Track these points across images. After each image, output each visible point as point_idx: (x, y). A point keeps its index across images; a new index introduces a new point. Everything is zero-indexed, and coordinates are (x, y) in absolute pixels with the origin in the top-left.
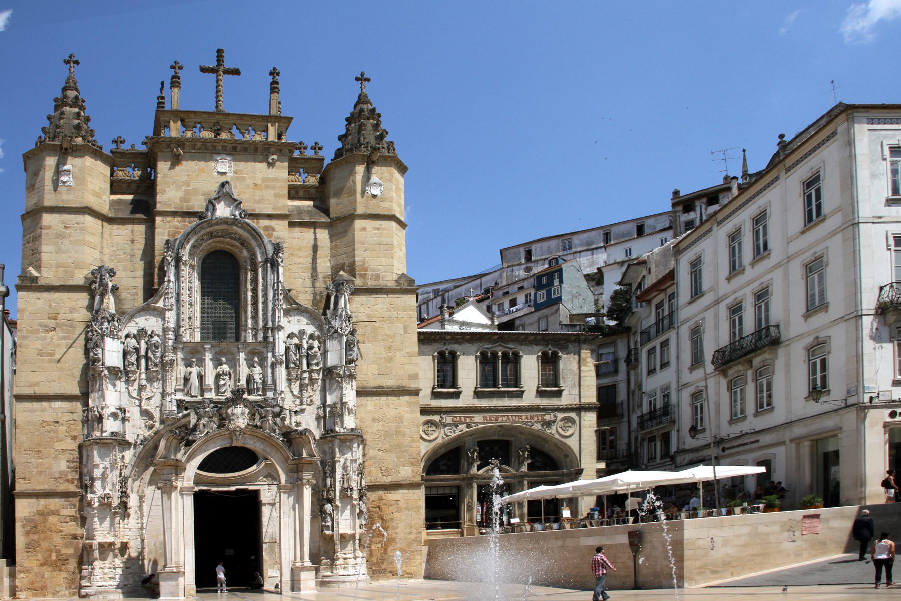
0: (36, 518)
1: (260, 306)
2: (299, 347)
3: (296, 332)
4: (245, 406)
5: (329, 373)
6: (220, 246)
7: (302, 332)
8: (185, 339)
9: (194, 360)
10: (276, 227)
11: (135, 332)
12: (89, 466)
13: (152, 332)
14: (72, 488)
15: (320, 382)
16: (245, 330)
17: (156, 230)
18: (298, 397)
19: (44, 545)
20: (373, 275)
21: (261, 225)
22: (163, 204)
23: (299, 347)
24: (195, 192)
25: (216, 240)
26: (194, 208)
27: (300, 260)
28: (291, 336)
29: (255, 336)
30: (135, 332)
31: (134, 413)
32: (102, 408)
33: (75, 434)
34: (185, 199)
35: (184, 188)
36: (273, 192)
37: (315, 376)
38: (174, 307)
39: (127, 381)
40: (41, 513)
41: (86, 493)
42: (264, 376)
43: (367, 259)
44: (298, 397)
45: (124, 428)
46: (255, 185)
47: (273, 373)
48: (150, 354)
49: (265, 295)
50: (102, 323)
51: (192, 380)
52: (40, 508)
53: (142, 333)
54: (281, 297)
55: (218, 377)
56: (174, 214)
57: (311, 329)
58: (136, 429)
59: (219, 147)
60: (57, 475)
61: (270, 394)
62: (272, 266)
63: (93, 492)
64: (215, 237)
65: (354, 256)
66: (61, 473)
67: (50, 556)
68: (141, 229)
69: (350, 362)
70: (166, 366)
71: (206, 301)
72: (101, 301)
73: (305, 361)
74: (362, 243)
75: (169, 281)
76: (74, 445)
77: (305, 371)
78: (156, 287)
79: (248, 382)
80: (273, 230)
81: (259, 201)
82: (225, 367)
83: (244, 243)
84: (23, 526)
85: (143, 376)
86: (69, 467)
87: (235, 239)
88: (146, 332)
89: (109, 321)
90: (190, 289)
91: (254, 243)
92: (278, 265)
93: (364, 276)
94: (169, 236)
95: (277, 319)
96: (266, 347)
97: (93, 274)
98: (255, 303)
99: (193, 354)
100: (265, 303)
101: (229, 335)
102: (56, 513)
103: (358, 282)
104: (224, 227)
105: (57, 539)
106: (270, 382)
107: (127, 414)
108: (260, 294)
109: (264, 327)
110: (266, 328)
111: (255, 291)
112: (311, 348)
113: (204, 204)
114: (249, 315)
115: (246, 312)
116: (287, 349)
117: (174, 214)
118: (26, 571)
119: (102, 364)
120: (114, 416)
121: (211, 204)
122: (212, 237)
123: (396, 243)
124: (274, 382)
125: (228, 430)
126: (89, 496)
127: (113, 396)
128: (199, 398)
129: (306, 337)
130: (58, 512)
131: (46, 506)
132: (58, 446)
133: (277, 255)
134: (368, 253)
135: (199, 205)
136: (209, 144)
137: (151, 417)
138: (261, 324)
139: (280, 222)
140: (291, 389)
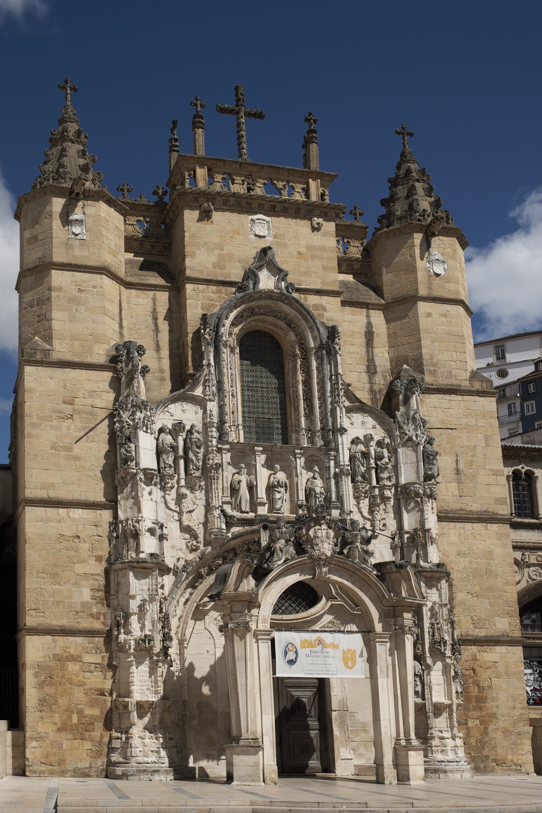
0: (52, 664)
1: (317, 403)
2: (366, 455)
4: (330, 527)
6: (260, 326)
8: (230, 440)
9: (243, 465)
12: (120, 596)
13: (192, 427)
14: (97, 625)
15: (392, 501)
16: (298, 432)
17: (188, 302)
18: (368, 519)
19: (63, 702)
21: (311, 301)
23: (366, 455)
24: (231, 258)
25: (257, 317)
26: (216, 276)
27: (354, 349)
28: (355, 441)
29: (311, 440)
30: (170, 426)
31: (172, 529)
32: (138, 521)
33: (101, 553)
34: (218, 265)
39: (163, 489)
40: (58, 658)
41: (119, 633)
42: (328, 490)
43: (436, 352)
44: (368, 519)
45: (161, 548)
46: (300, 253)
48: (191, 455)
49: (322, 389)
50: (133, 414)
51: (241, 492)
52: (57, 651)
53: (178, 427)
54: (342, 393)
55: (271, 489)
56: (208, 282)
57: (379, 434)
58: (176, 550)
59: (255, 205)
60: (79, 608)
62: (329, 353)
63: (128, 632)
64: (257, 314)
65: (420, 347)
66: (83, 604)
67: (70, 717)
68: (163, 297)
70: (209, 472)
71: (246, 393)
72: (130, 383)
73: (373, 472)
75: (209, 365)
76: (99, 568)
77: (375, 487)
78: (191, 371)
79: (307, 497)
80: (324, 309)
82: (281, 476)
83: (290, 324)
84: (36, 675)
85: (183, 482)
87: (279, 318)
88: (184, 428)
91: (303, 324)
92: (336, 353)
93: (433, 373)
94: (203, 309)
95: (339, 420)
97: (116, 349)
98: (309, 399)
99: (242, 456)
100: (323, 397)
101: (275, 437)
102: (77, 659)
104: (269, 302)
105: (79, 694)
106: (334, 498)
107: (165, 531)
108: (315, 387)
109: (322, 429)
111: (307, 383)
112: (379, 457)
113: (242, 273)
114: (302, 412)
115: (297, 409)
116: (352, 458)
117: (208, 282)
118: (40, 738)
119: (136, 463)
120: (152, 531)
121: (251, 275)
123: (465, 335)
124: (340, 498)
125: (311, 557)
126: (122, 637)
127: (151, 506)
128: (251, 515)
129: (373, 443)
130: (80, 657)
132: (80, 569)
133: (333, 342)
134: (437, 344)
135: (237, 275)
136: (244, 201)
137: (195, 536)
140: (359, 509)
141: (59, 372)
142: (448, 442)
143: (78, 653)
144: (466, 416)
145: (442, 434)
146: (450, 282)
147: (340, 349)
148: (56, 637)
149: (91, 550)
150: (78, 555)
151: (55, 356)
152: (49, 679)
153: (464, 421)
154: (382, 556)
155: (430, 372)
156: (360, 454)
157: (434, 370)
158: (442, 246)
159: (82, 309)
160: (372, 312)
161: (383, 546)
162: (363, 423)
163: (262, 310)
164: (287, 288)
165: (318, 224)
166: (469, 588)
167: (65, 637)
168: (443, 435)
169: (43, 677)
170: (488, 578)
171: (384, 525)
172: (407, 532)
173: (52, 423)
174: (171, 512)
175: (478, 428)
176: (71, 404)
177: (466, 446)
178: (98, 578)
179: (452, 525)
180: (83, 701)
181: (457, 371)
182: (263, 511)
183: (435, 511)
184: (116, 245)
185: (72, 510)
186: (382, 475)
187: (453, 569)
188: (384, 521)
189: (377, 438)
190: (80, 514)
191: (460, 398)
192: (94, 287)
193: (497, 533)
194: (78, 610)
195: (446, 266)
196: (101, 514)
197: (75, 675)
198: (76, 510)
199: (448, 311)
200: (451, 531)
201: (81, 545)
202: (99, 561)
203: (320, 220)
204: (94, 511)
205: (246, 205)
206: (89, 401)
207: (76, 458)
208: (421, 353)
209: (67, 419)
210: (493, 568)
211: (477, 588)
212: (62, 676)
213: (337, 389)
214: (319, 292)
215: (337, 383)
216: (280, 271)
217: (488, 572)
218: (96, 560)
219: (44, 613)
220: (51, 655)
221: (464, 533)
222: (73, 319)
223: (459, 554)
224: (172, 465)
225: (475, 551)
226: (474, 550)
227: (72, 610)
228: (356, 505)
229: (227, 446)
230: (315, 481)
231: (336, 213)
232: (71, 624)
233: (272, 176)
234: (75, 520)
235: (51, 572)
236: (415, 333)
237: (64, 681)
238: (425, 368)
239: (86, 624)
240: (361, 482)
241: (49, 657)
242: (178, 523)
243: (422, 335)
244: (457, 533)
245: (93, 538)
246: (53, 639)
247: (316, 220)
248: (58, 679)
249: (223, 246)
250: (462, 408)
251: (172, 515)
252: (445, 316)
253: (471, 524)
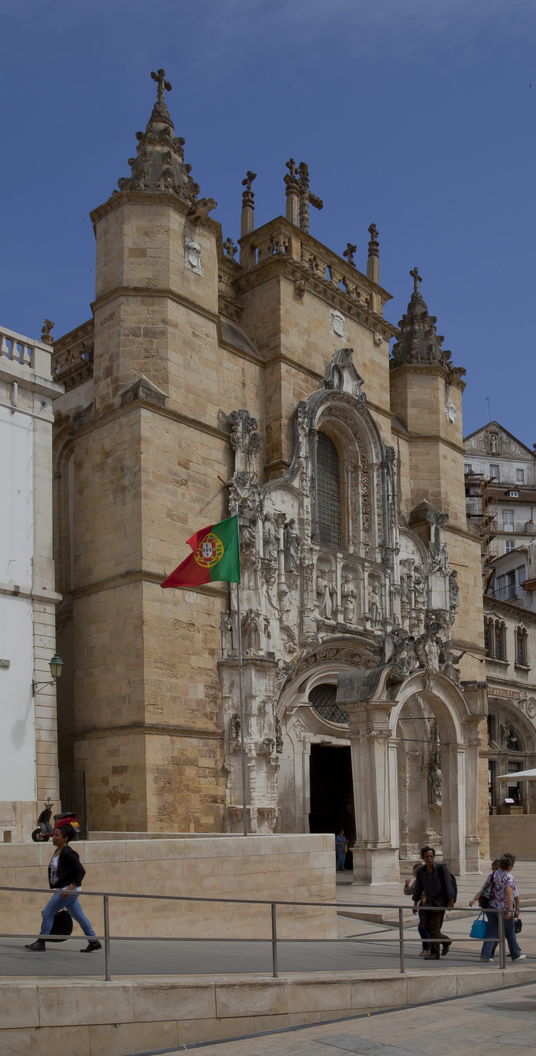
0: (171, 768)
2: (409, 577)
33: (213, 646)
52: (176, 754)
55: (345, 597)
60: (194, 706)
69: (453, 607)
76: (210, 663)
85: (283, 579)
86: (206, 697)
96: (385, 572)
102: (193, 763)
105: (195, 801)
128: (333, 622)
131: (182, 751)
132: (196, 662)
143: (194, 756)
148: (174, 738)
149: (205, 641)
150: (193, 646)
152: (168, 785)
167: (183, 738)
169: (162, 783)
174: (272, 609)
178: (211, 674)
180: (198, 809)
182: (341, 619)
185: (187, 592)
186: (419, 599)
194: (193, 708)
196: (213, 602)
197: (191, 780)
201: (196, 634)
202: (212, 655)
206: (202, 469)
212: (180, 782)
218: (209, 654)
219: (162, 709)
220: (170, 759)
227: (189, 707)
232: (188, 724)
235: (168, 663)
237: (182, 787)
239: (202, 724)
241: (168, 759)
242: (278, 622)
245: (206, 628)
246: (171, 740)
248: (177, 785)
251: (273, 612)
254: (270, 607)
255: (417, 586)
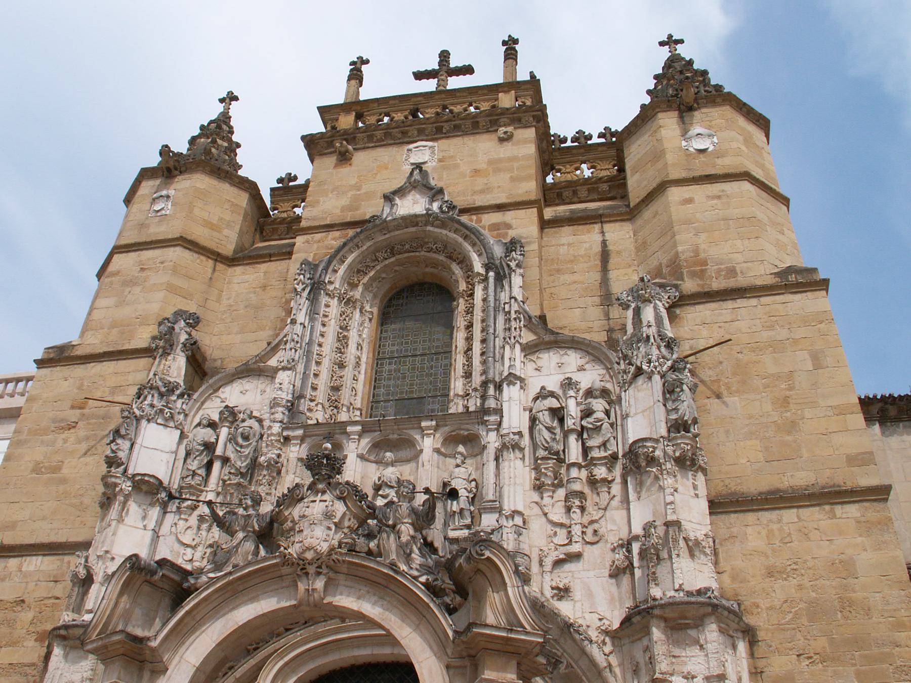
2: (558, 414)
3: (553, 384)
5: (638, 462)
7: (568, 384)
10: (514, 223)
11: (216, 417)
20: (720, 270)
22: (314, 219)
24: (369, 196)
28: (544, 394)
35: (350, 194)
36: (506, 176)
37: (601, 472)
38: (300, 368)
43: (702, 247)
44: (562, 525)
46: (476, 172)
47: (498, 475)
56: (329, 227)
61: (488, 521)
65: (675, 245)
69: (679, 426)
74: (688, 222)
75: (293, 322)
80: (508, 226)
81: (482, 192)
89: (161, 395)
90: (342, 340)
93: (701, 274)
103: (689, 286)
110: (485, 384)
116: (533, 420)
117: (329, 227)
122: (393, 254)
134: (703, 236)
135: (372, 208)
138: (477, 379)
139: (521, 213)
141: (79, 371)
142: (734, 374)
144: (771, 328)
145: (721, 363)
146: (723, 156)
147: (518, 266)
151: (79, 352)
153: (765, 335)
154: (590, 595)
155: (693, 275)
156: (547, 413)
157: (702, 271)
158: (708, 119)
159: (137, 290)
160: (607, 227)
161: (591, 574)
162: (560, 365)
163: (407, 246)
164: (441, 208)
165: (505, 133)
166: (801, 642)
168: (724, 364)
170: (846, 618)
171: (595, 531)
172: (636, 538)
173: (45, 438)
175: (796, 342)
176: (80, 408)
177: (772, 375)
179: (750, 517)
181: (745, 265)
183: (702, 491)
184: (221, 219)
186: (590, 443)
187: (758, 607)
188: (596, 526)
189: (584, 386)
190: (38, 564)
191: (754, 302)
192: (162, 263)
193: (858, 522)
195: (715, 139)
196: (69, 562)
198: (34, 558)
199: (723, 191)
200: (749, 530)
203: (510, 129)
204: (61, 557)
205: (399, 136)
207: (64, 481)
208: (677, 253)
209: (69, 429)
210: (859, 595)
211: (821, 643)
213: (510, 320)
214: (500, 208)
215: (509, 312)
216: (431, 189)
217: (847, 604)
221: (781, 530)
222: (121, 303)
223: (770, 573)
224: (202, 472)
225: (809, 564)
226: (805, 562)
228: (537, 503)
229: (300, 432)
230: (457, 470)
231: (534, 117)
233: (445, 103)
234: (26, 575)
236: (668, 230)
238: (685, 271)
240: (543, 459)
243: (676, 228)
244: (764, 533)
245: (46, 601)
247: (502, 130)
249: (361, 186)
250: (759, 316)
252: (719, 197)
253: (795, 510)
254: (177, 546)
255: (584, 423)
